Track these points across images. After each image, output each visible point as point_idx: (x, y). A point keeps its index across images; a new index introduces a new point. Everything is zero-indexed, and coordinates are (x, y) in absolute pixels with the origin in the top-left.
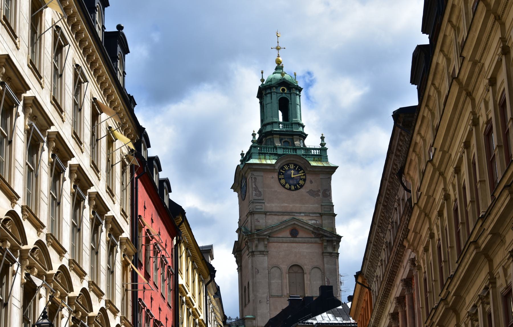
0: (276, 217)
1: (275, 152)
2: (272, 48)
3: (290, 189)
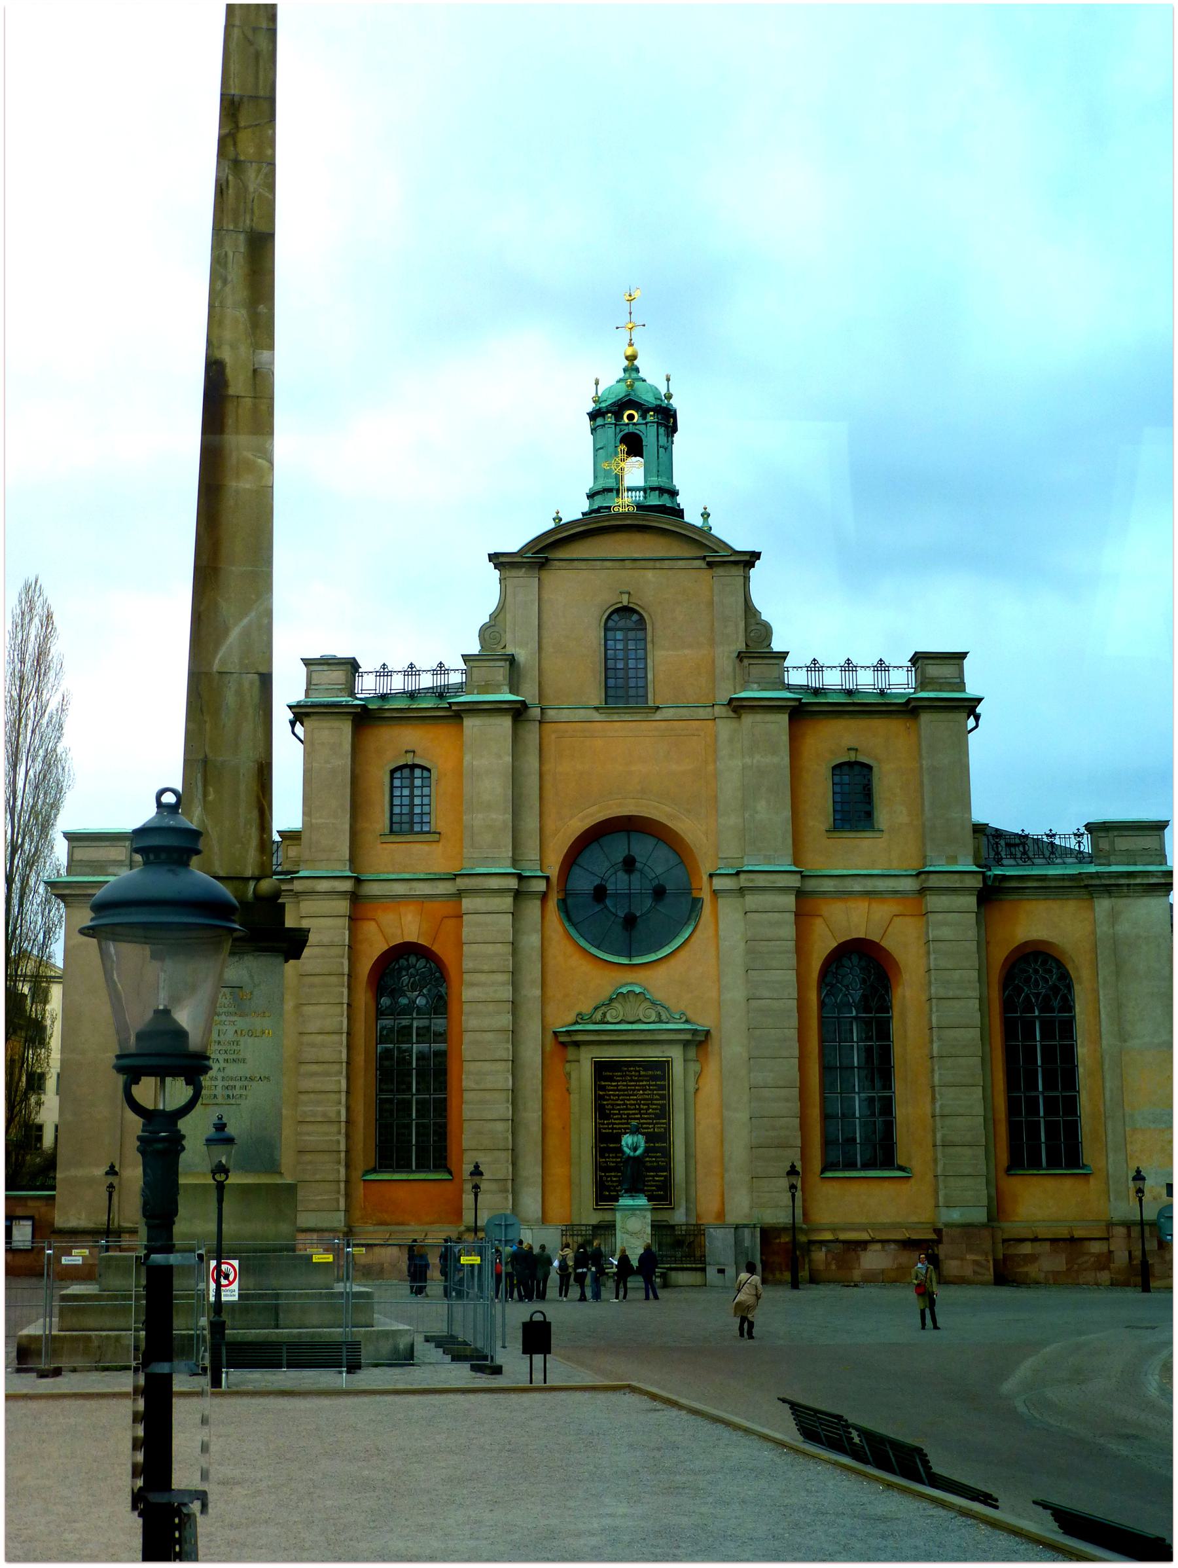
2: (617, 328)
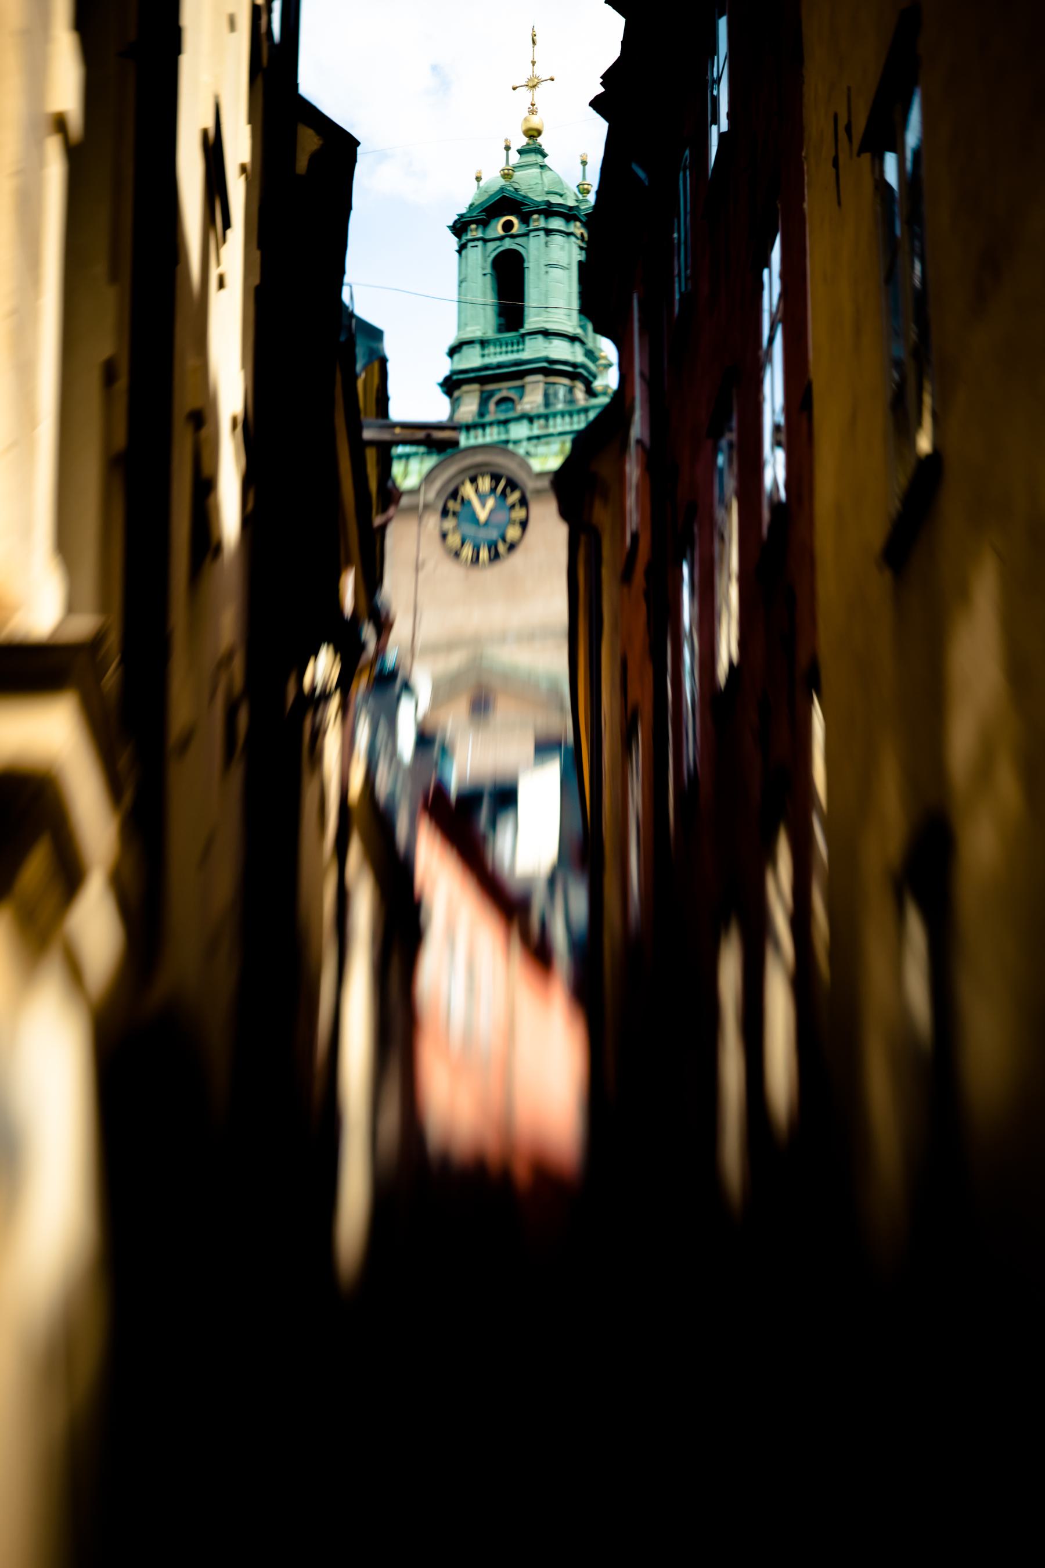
2: (514, 89)
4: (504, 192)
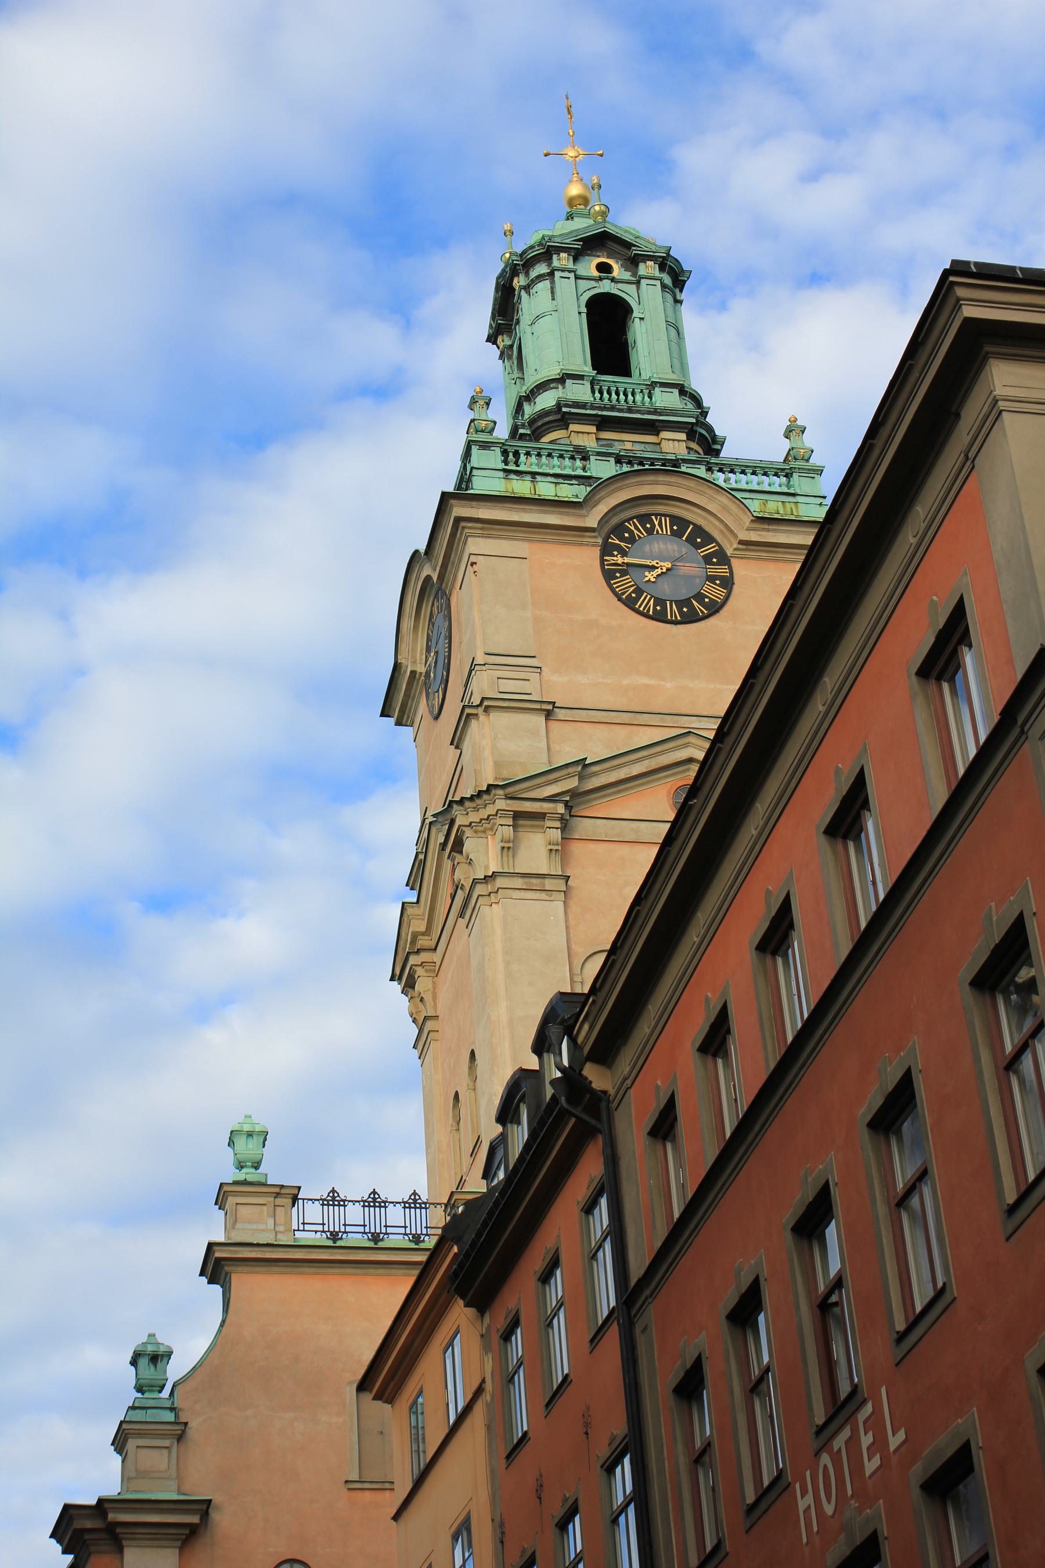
0: (601, 731)
1: (580, 472)
3: (660, 617)
4: (605, 227)
